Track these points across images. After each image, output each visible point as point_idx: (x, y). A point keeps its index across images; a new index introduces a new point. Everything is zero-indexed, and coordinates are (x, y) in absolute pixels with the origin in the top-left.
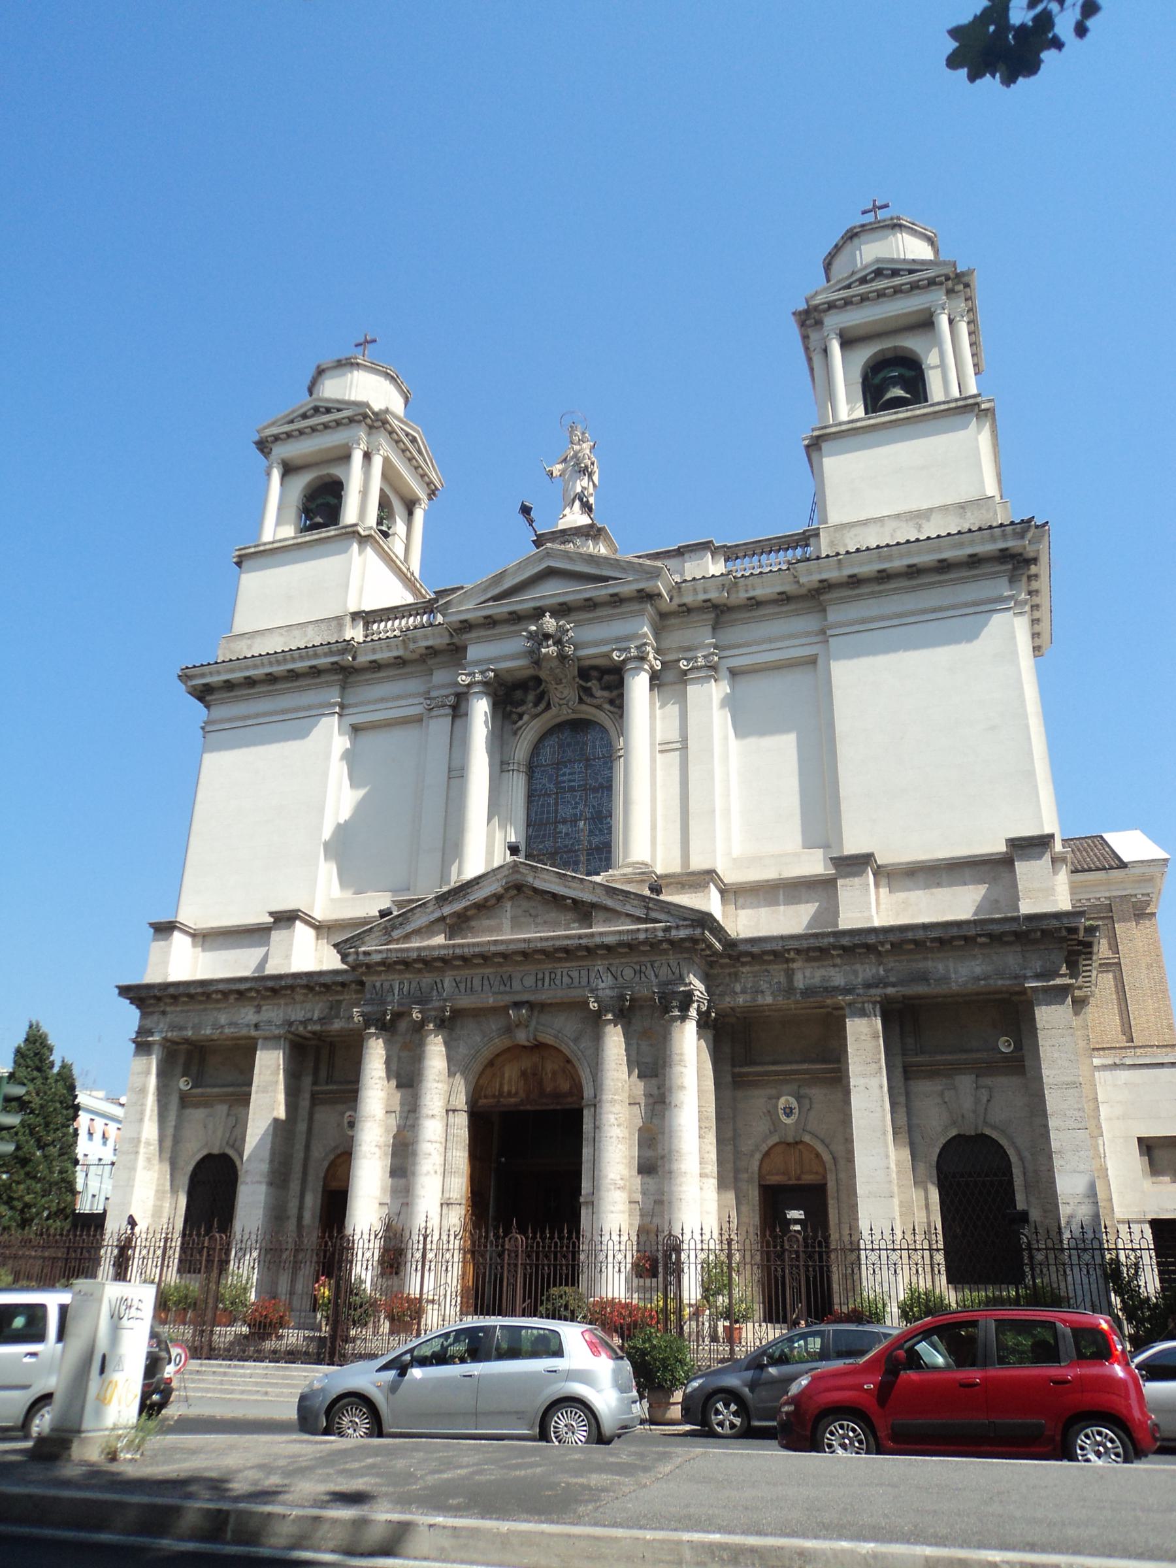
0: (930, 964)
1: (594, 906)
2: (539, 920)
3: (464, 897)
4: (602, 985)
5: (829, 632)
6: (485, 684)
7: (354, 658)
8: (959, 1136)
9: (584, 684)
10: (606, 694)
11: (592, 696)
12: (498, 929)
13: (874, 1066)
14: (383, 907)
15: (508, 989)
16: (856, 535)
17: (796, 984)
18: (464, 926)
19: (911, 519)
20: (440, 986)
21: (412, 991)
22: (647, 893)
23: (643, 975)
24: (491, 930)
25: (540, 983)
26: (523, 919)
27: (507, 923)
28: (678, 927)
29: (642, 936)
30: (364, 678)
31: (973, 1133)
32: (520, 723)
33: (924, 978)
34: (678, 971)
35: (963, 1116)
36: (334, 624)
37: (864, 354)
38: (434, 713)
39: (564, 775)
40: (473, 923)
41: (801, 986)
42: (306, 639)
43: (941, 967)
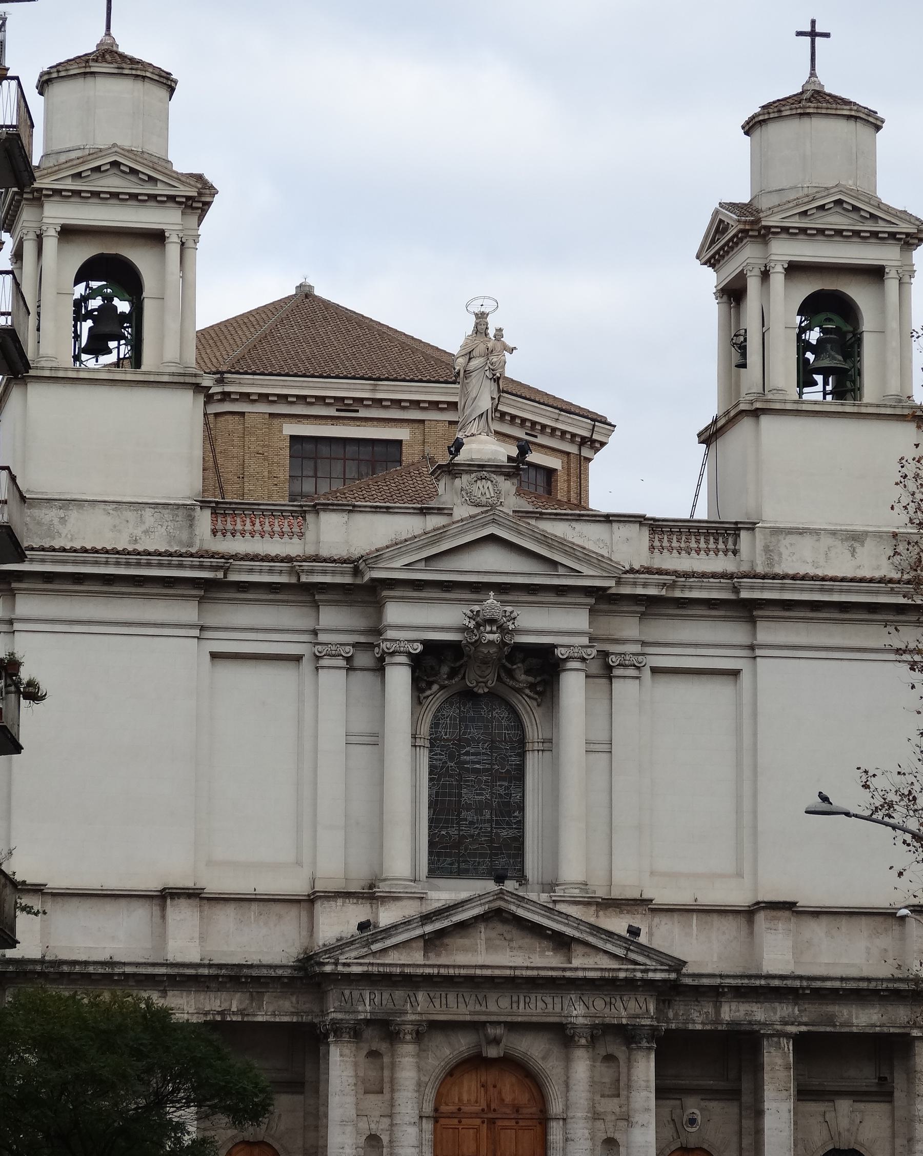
0: (837, 1008)
1: (573, 939)
2: (514, 944)
3: (447, 917)
4: (575, 1013)
5: (758, 652)
6: (409, 654)
7: (225, 576)
8: (834, 1149)
9: (509, 666)
10: (531, 679)
11: (513, 678)
12: (474, 950)
13: (785, 1093)
14: (363, 919)
15: (484, 1009)
16: (791, 544)
17: (722, 1016)
18: (437, 943)
19: (847, 539)
20: (413, 999)
21: (384, 1002)
22: (624, 933)
23: (612, 1006)
24: (466, 950)
25: (515, 1005)
26: (498, 942)
27: (481, 944)
28: (655, 970)
29: (622, 975)
30: (226, 595)
31: (846, 1149)
32: (428, 693)
33: (830, 1020)
34: (644, 1007)
35: (840, 1134)
36: (181, 512)
37: (805, 289)
38: (325, 662)
39: (467, 753)
40: (446, 941)
41: (727, 1018)
42: (144, 528)
43: (845, 1012)
